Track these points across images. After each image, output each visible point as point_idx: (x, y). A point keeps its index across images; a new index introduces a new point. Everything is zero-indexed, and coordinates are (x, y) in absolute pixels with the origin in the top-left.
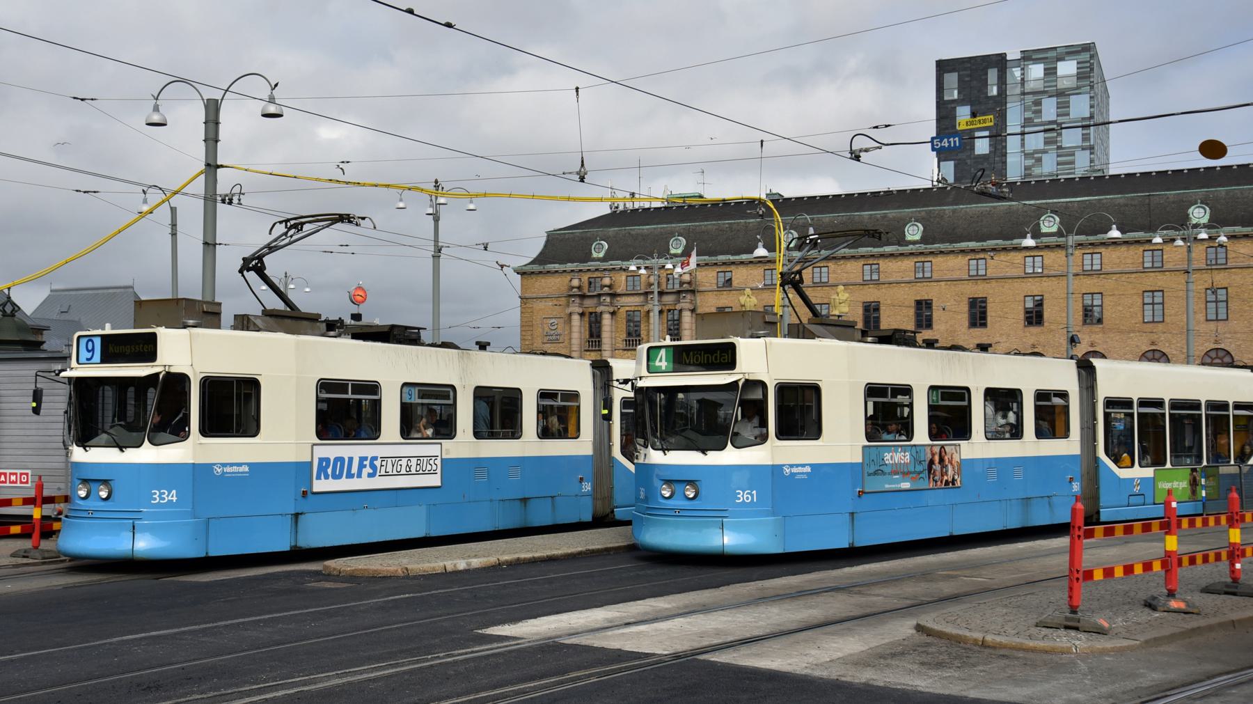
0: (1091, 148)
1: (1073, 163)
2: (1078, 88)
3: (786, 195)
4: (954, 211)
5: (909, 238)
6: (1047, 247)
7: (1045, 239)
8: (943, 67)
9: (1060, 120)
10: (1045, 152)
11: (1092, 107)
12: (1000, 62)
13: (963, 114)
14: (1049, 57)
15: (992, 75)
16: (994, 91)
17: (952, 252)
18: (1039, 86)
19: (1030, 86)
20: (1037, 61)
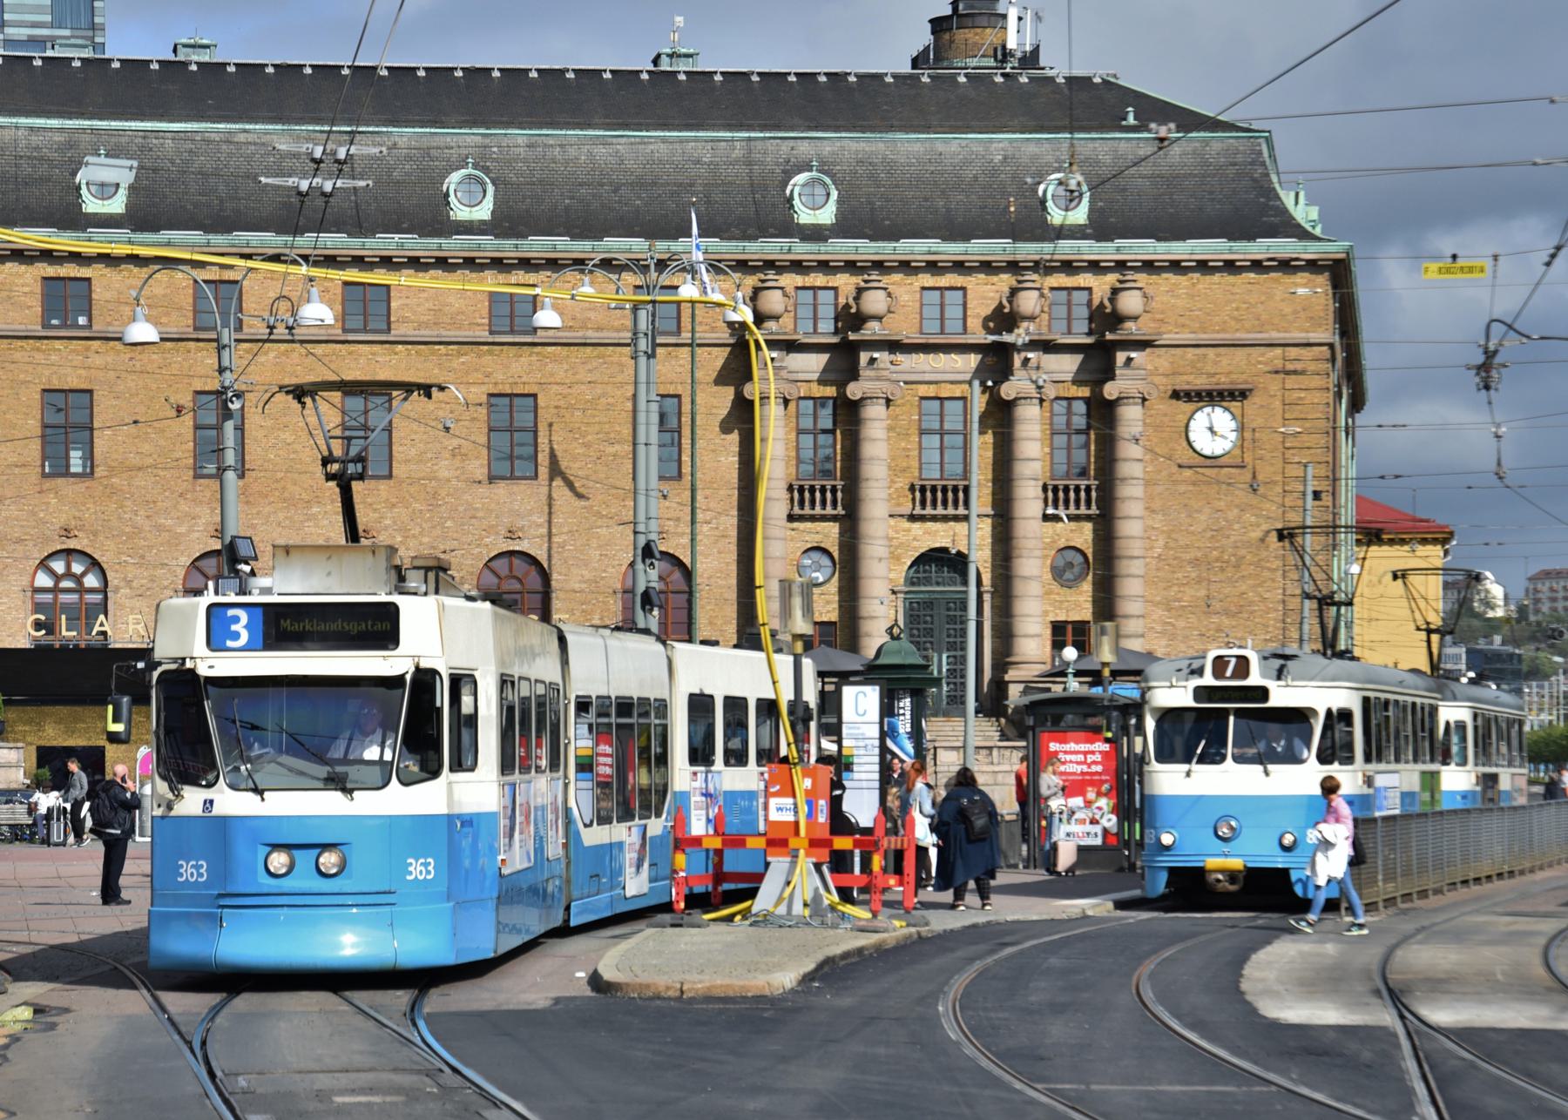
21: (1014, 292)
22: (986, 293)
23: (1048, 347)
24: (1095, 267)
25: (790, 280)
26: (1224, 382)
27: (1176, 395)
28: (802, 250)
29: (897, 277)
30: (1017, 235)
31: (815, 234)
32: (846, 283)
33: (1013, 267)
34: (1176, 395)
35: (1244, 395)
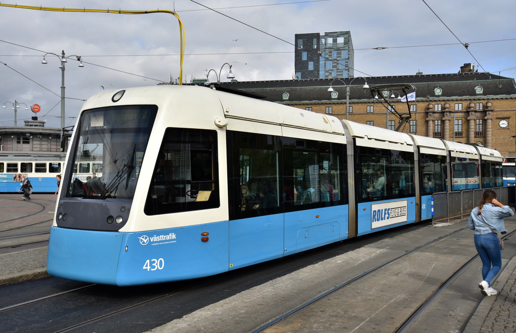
0: (348, 70)
1: (342, 75)
2: (344, 47)
3: (239, 81)
4: (301, 89)
5: (284, 98)
6: (334, 103)
7: (333, 101)
8: (298, 37)
9: (338, 59)
10: (333, 70)
11: (349, 55)
12: (317, 36)
13: (305, 56)
14: (335, 35)
15: (315, 41)
16: (315, 47)
17: (300, 104)
18: (331, 46)
19: (328, 46)
20: (330, 37)
21: (470, 104)
22: (466, 104)
23: (476, 111)
24: (483, 99)
25: (434, 103)
26: (505, 116)
27: (497, 118)
28: (436, 98)
29: (451, 102)
30: (471, 95)
31: (438, 96)
32: (443, 103)
33: (470, 100)
34: (497, 118)
35: (509, 118)
